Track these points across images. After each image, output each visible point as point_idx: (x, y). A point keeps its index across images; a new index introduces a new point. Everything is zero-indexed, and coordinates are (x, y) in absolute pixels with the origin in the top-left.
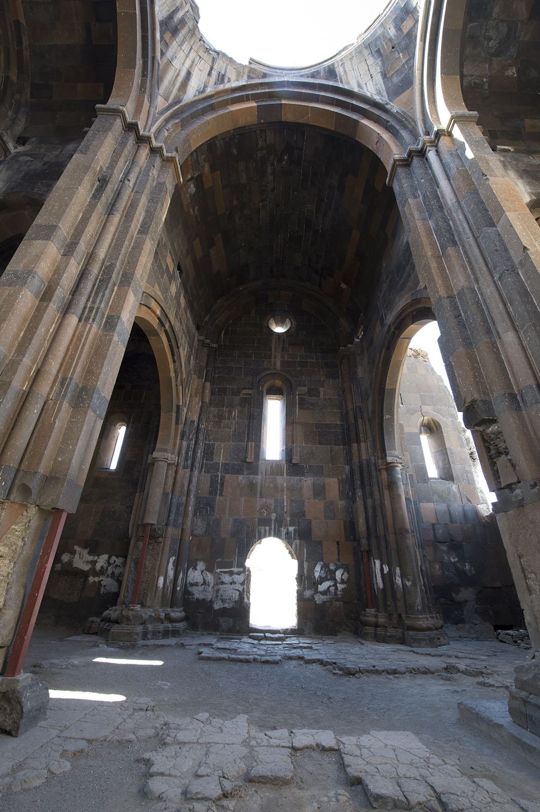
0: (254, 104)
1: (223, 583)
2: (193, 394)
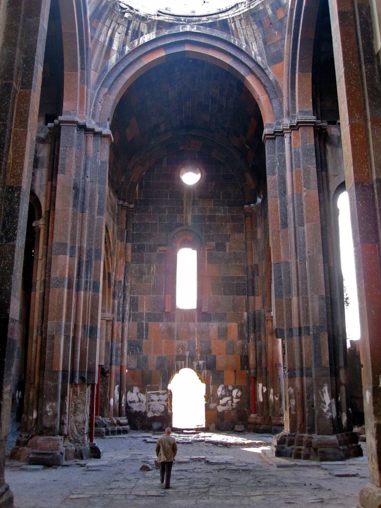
0: (162, 54)
1: (152, 401)
2: (118, 258)
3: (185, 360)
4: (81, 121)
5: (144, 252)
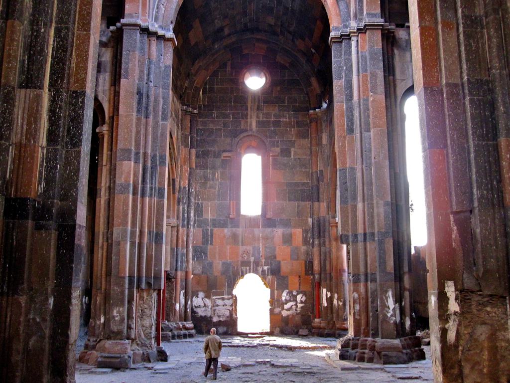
1: (217, 305)
3: (250, 266)
4: (143, 24)
5: (208, 158)
